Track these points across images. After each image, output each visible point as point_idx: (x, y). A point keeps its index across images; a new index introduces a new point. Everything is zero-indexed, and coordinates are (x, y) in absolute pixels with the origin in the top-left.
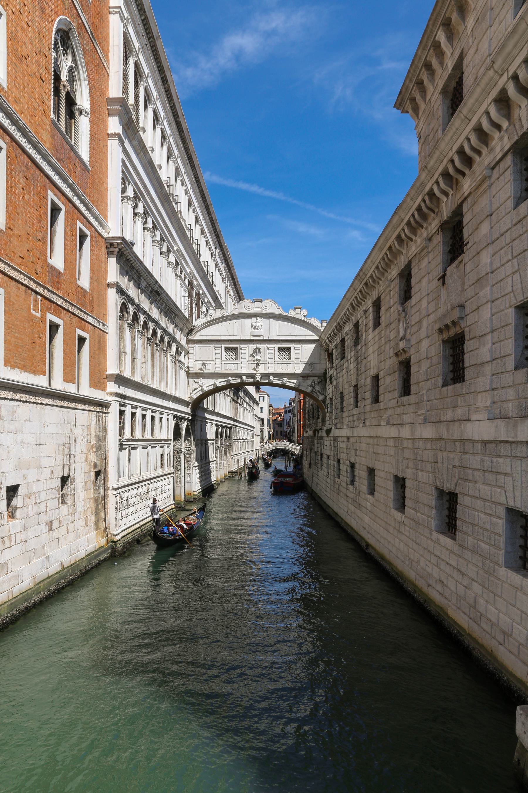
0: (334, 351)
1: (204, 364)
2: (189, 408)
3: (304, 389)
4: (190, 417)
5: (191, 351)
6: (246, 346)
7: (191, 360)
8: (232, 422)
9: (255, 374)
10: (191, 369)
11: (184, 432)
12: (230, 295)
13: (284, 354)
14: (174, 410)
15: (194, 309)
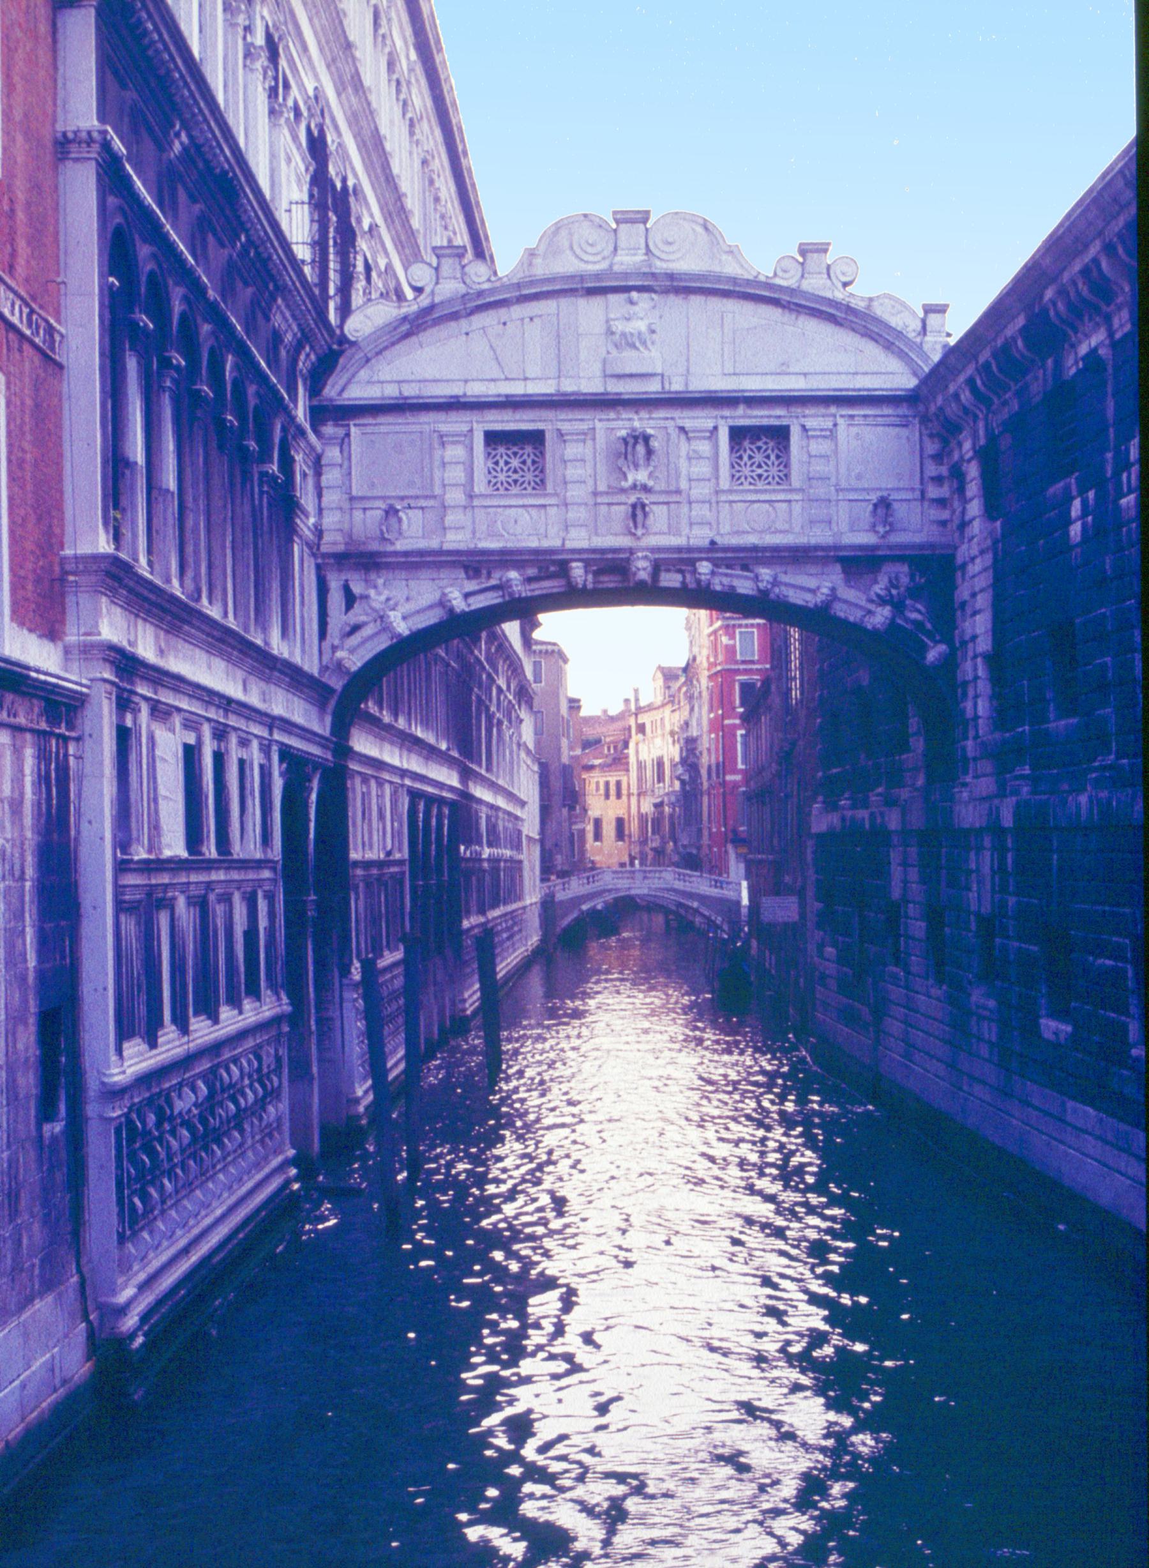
0: (1005, 443)
1: (391, 512)
2: (328, 720)
3: (854, 616)
4: (329, 756)
5: (333, 454)
6: (584, 426)
7: (331, 498)
8: (454, 780)
9: (631, 551)
10: (327, 538)
11: (312, 825)
12: (437, 200)
13: (759, 458)
14: (287, 725)
15: (331, 257)
